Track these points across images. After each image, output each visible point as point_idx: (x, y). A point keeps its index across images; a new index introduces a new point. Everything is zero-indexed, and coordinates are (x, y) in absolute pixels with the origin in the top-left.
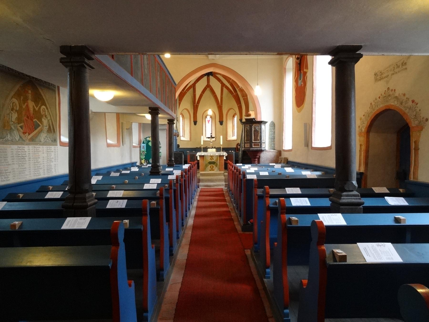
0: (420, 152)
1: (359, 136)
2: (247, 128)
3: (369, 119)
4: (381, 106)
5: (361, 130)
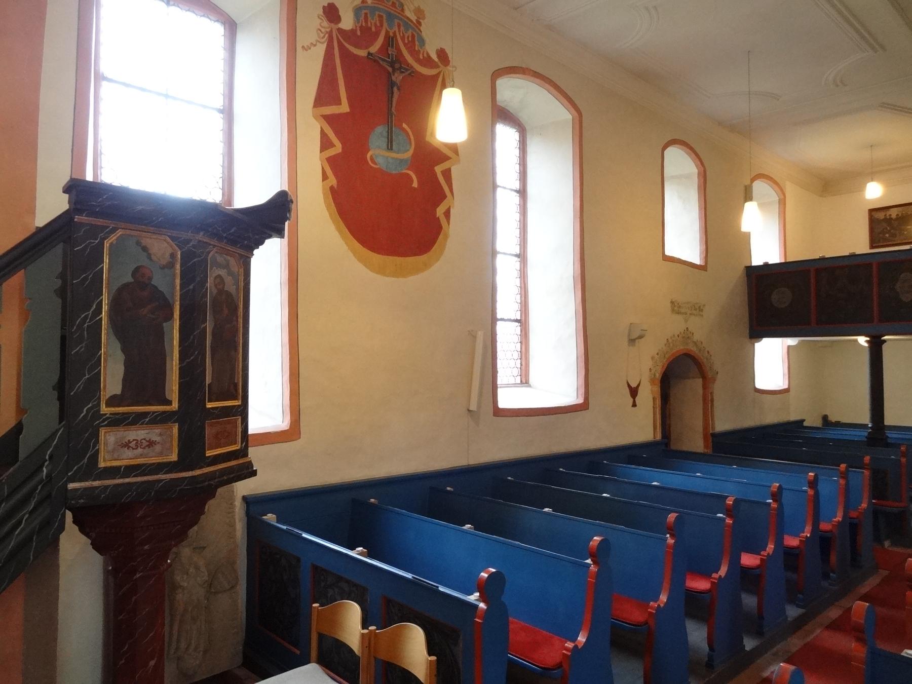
0: (715, 403)
1: (651, 385)
2: (222, 272)
3: (665, 361)
4: (682, 348)
5: (655, 375)
